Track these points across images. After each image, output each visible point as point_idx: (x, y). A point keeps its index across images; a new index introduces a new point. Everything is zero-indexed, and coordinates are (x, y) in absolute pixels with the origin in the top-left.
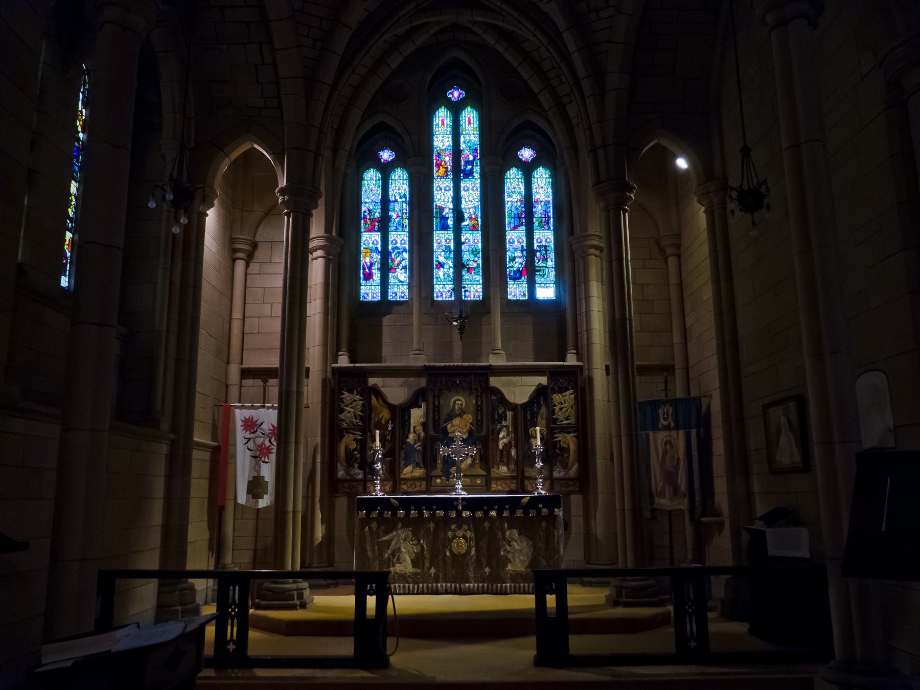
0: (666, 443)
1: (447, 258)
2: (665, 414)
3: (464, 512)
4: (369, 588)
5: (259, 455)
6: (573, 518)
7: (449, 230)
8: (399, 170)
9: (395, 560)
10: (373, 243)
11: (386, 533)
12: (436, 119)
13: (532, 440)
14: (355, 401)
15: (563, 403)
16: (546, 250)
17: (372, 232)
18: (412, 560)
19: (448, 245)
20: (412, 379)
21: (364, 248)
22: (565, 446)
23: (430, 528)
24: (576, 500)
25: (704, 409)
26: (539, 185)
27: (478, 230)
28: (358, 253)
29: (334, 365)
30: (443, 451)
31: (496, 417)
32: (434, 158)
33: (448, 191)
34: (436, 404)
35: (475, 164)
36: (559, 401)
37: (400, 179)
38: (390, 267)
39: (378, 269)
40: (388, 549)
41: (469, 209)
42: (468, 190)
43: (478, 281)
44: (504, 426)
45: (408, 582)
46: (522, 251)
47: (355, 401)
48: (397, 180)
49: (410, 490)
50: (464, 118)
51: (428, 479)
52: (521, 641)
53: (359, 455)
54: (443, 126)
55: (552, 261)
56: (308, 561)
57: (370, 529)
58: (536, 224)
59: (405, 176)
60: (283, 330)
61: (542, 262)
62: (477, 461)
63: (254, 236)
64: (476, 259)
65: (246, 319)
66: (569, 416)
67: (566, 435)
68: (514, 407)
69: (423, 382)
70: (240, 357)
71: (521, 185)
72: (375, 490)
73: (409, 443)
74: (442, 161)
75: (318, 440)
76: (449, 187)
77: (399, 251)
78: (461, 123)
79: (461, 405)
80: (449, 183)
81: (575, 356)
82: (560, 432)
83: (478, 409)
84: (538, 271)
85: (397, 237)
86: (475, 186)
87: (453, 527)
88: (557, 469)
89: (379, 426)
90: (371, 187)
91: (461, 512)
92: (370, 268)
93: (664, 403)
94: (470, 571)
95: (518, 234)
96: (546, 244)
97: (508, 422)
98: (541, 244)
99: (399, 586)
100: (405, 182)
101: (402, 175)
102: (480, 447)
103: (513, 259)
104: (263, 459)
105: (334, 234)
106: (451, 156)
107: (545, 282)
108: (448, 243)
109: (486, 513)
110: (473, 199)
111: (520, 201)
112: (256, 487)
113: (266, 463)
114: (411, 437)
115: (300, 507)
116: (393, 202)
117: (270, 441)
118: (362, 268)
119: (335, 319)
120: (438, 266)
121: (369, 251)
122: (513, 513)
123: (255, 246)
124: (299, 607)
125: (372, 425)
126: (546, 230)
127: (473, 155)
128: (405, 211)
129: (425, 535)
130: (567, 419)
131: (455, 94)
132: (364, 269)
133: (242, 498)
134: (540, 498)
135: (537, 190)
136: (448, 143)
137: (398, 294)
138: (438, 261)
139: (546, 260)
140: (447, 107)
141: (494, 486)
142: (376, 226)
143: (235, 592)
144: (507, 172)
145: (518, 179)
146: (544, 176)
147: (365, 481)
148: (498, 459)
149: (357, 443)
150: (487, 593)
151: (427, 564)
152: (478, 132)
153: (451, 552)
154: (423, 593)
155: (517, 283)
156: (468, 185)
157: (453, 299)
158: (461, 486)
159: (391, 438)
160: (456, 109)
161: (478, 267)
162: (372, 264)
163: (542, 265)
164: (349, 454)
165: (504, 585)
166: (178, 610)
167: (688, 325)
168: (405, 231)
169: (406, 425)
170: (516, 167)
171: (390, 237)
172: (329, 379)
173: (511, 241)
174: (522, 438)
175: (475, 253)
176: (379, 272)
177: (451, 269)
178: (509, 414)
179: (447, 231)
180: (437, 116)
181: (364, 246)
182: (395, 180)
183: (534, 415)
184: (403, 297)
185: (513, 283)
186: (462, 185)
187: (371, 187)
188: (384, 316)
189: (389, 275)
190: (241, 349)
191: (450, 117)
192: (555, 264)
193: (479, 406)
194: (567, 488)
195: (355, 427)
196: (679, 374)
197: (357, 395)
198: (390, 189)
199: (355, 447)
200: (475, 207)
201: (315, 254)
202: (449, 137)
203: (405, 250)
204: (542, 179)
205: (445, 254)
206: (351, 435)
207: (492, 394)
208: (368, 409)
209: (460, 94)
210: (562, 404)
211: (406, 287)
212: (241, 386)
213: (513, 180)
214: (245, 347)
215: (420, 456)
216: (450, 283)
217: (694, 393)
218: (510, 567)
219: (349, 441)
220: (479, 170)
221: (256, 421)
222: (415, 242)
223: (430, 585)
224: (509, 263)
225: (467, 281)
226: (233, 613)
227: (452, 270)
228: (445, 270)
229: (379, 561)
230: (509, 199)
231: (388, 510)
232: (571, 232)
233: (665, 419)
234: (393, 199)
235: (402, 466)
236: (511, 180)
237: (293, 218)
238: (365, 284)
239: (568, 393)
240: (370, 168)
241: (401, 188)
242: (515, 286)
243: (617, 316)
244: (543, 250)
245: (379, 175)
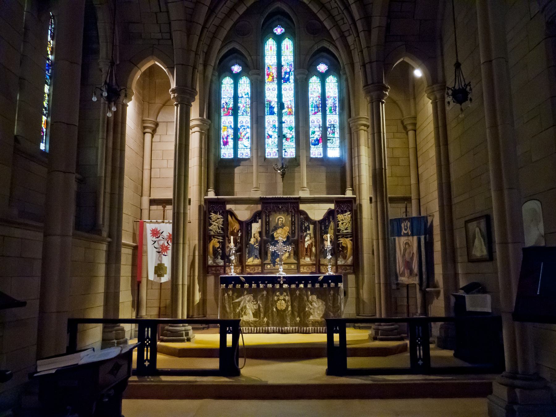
0: (406, 244)
2: (405, 226)
3: (284, 285)
4: (228, 329)
5: (161, 251)
6: (349, 289)
9: (243, 313)
10: (229, 123)
11: (238, 297)
13: (325, 242)
14: (218, 219)
15: (344, 220)
16: (334, 127)
18: (253, 314)
20: (253, 205)
22: (345, 245)
23: (264, 294)
24: (351, 278)
25: (429, 224)
27: (292, 115)
28: (219, 129)
29: (205, 197)
30: (272, 249)
31: (304, 228)
32: (266, 70)
34: (267, 221)
35: (291, 74)
36: (341, 219)
39: (232, 139)
40: (239, 306)
41: (287, 102)
42: (286, 90)
44: (308, 234)
45: (251, 326)
46: (319, 127)
47: (218, 219)
49: (252, 272)
50: (284, 45)
51: (263, 265)
52: (318, 360)
53: (221, 251)
56: (191, 314)
57: (228, 295)
59: (248, 82)
60: (175, 176)
62: (292, 255)
63: (156, 119)
64: (291, 132)
65: (152, 169)
66: (347, 228)
67: (345, 239)
68: (314, 223)
69: (259, 207)
70: (149, 192)
72: (231, 272)
73: (251, 244)
75: (197, 242)
76: (275, 88)
77: (244, 127)
78: (282, 48)
79: (283, 221)
80: (275, 86)
81: (351, 191)
82: (342, 237)
83: (293, 223)
84: (329, 140)
87: (278, 294)
88: (340, 260)
89: (233, 233)
90: (227, 88)
91: (282, 285)
92: (227, 138)
93: (405, 220)
94: (288, 320)
95: (317, 117)
97: (311, 231)
99: (246, 329)
100: (248, 85)
101: (246, 81)
102: (294, 246)
104: (163, 254)
105: (205, 117)
107: (333, 147)
108: (274, 123)
109: (297, 286)
111: (318, 97)
112: (159, 270)
113: (166, 255)
114: (252, 241)
115: (186, 283)
117: (168, 243)
119: (206, 169)
120: (269, 137)
121: (226, 128)
122: (313, 285)
123: (157, 125)
124: (186, 341)
125: (229, 233)
128: (248, 103)
129: (261, 298)
130: (346, 229)
131: (279, 31)
132: (223, 139)
133: (152, 276)
134: (330, 277)
135: (329, 90)
138: (268, 134)
139: (334, 133)
141: (302, 270)
142: (231, 113)
143: (148, 332)
145: (317, 83)
146: (333, 81)
147: (225, 267)
148: (305, 253)
149: (220, 244)
150: (298, 333)
151: (262, 315)
152: (293, 54)
153: (276, 308)
154: (260, 333)
156: (286, 87)
157: (277, 157)
158: (282, 270)
159: (241, 240)
160: (279, 40)
161: (292, 138)
162: (228, 136)
164: (215, 250)
165: (308, 328)
166: (115, 342)
167: (420, 173)
169: (249, 233)
170: (316, 76)
171: (239, 119)
172: (203, 206)
173: (313, 121)
174: (319, 241)
176: (232, 140)
178: (311, 227)
180: (267, 44)
183: (327, 227)
184: (247, 156)
188: (235, 168)
190: (149, 188)
192: (340, 136)
193: (293, 222)
194: (345, 270)
195: (219, 234)
196: (414, 202)
197: (219, 215)
198: (239, 90)
199: (218, 246)
201: (194, 130)
202: (274, 57)
203: (248, 127)
204: (332, 82)
206: (216, 239)
207: (301, 215)
208: (226, 223)
209: (282, 30)
210: (343, 220)
212: (150, 210)
213: (314, 83)
214: (151, 186)
215: (258, 252)
216: (275, 147)
217: (422, 215)
218: (311, 317)
219: (215, 243)
221: (159, 230)
222: (254, 123)
223: (264, 328)
224: (312, 135)
225: (286, 146)
226: (147, 344)
227: (276, 140)
229: (234, 313)
230: (312, 96)
231: (239, 284)
232: (350, 116)
233: (405, 230)
234: (241, 96)
235: (247, 258)
237: (180, 107)
239: (346, 214)
240: (227, 76)
242: (315, 149)
243: (377, 167)
245: (232, 81)
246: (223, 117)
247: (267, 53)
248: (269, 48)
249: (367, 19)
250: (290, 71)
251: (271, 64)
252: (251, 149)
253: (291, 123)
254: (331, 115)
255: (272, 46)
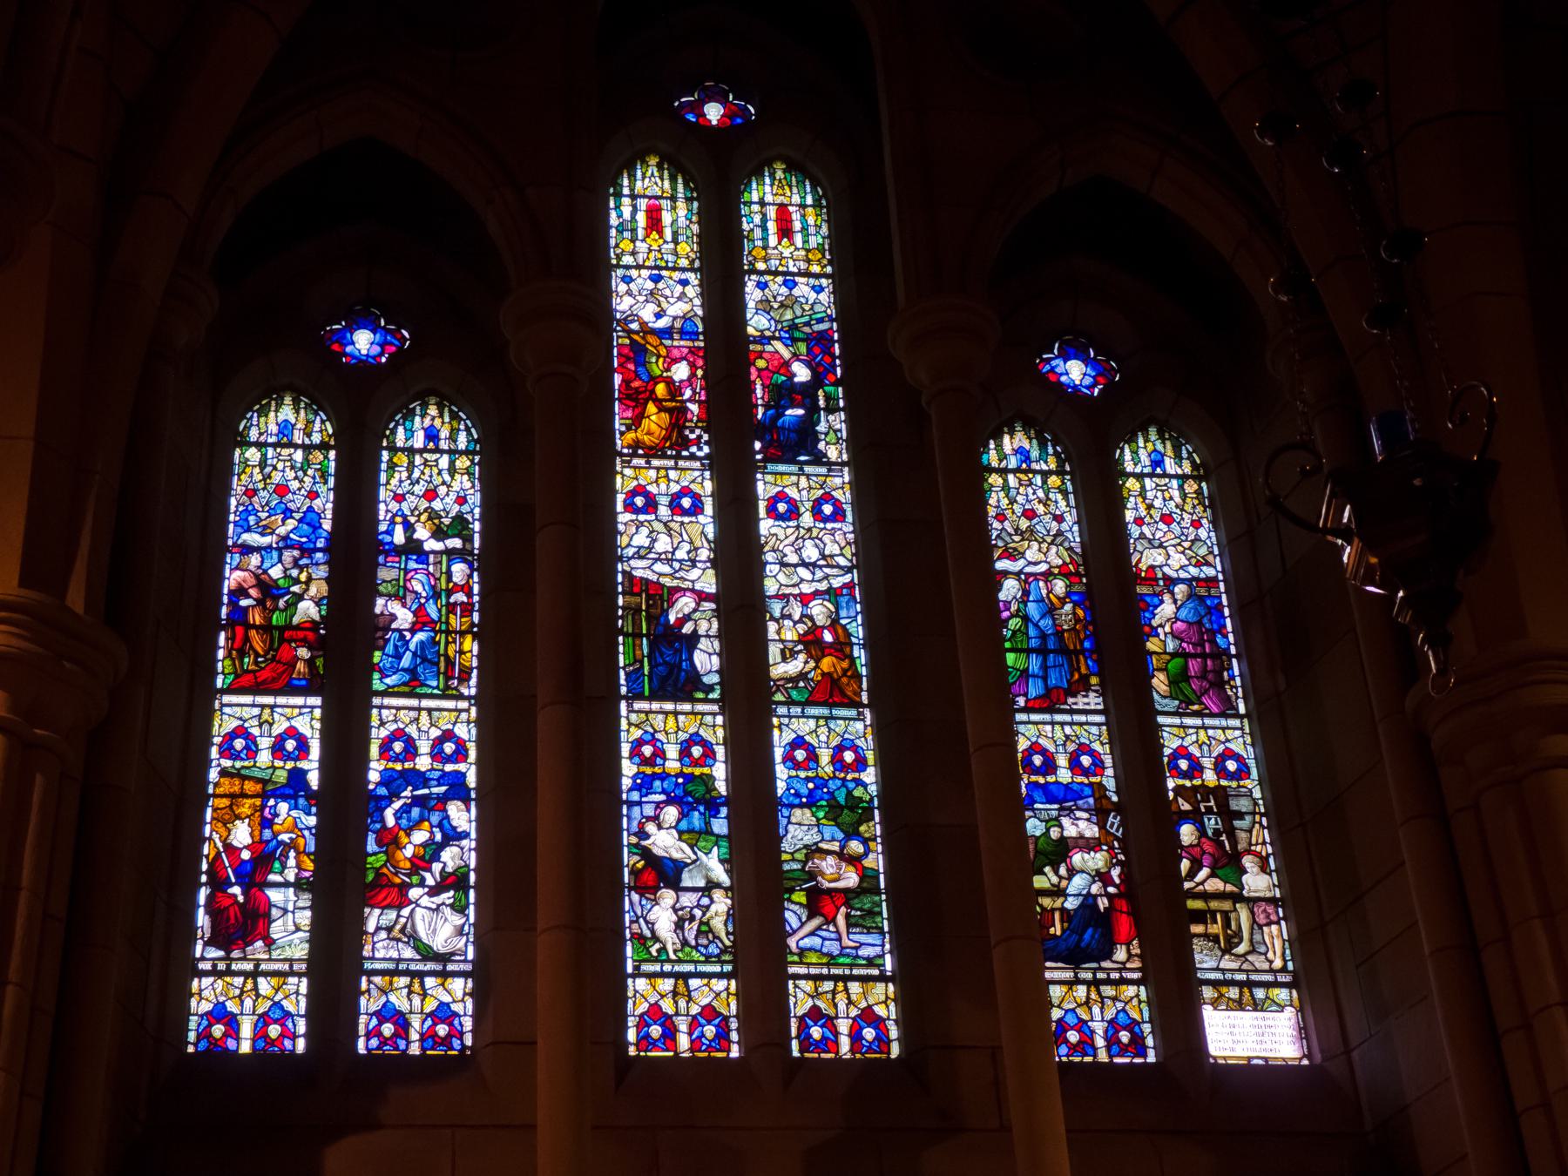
1: (692, 837)
7: (700, 695)
8: (433, 411)
10: (278, 749)
12: (617, 207)
16: (1229, 816)
17: (276, 693)
19: (697, 771)
21: (224, 773)
26: (1150, 507)
27: (857, 705)
33: (685, 512)
35: (822, 403)
37: (437, 450)
38: (371, 876)
39: (299, 885)
42: (793, 513)
43: (870, 962)
46: (1100, 814)
48: (421, 451)
50: (756, 208)
54: (655, 235)
55: (1264, 868)
58: (1160, 682)
61: (1213, 875)
64: (855, 847)
71: (1062, 504)
74: (655, 380)
76: (697, 499)
78: (745, 226)
84: (1200, 917)
85: (417, 719)
86: (827, 498)
92: (256, 870)
95: (1068, 730)
96: (1224, 783)
98: (1197, 782)
100: (463, 463)
101: (444, 433)
103: (1060, 851)
105: (76, 598)
106: (700, 363)
110: (824, 557)
116: (398, 551)
118: (204, 878)
120: (649, 878)
126: (1212, 715)
127: (808, 364)
128: (460, 597)
132: (218, 883)
135: (1145, 529)
136: (687, 307)
137: (416, 1022)
138: (646, 853)
139: (1229, 863)
140: (674, 165)
142: (300, 666)
144: (987, 445)
145: (1045, 475)
155: (1089, 976)
156: (792, 493)
162: (265, 856)
163: (1215, 885)
168: (461, 697)
171: (375, 721)
175: (847, 817)
176: (305, 900)
177: (718, 895)
179: (694, 701)
180: (626, 191)
181: (227, 763)
182: (411, 451)
185: (1068, 975)
186: (764, 488)
187: (277, 478)
189: (362, 921)
191: (689, 200)
200: (832, 594)
202: (684, 283)
203: (457, 788)
205: (683, 815)
211: (458, 985)
216: (717, 968)
220: (838, 421)
227: (721, 904)
228: (688, 900)
236: (1011, 477)
238: (221, 966)
241: (442, 490)
242: (1081, 991)
244: (1209, 811)
245: (322, 429)
246: (226, 699)
247: (626, 245)
248: (641, 218)
250: (817, 381)
251: (662, 323)
252: (483, 978)
253: (845, 767)
254: (1188, 721)
255: (665, 204)
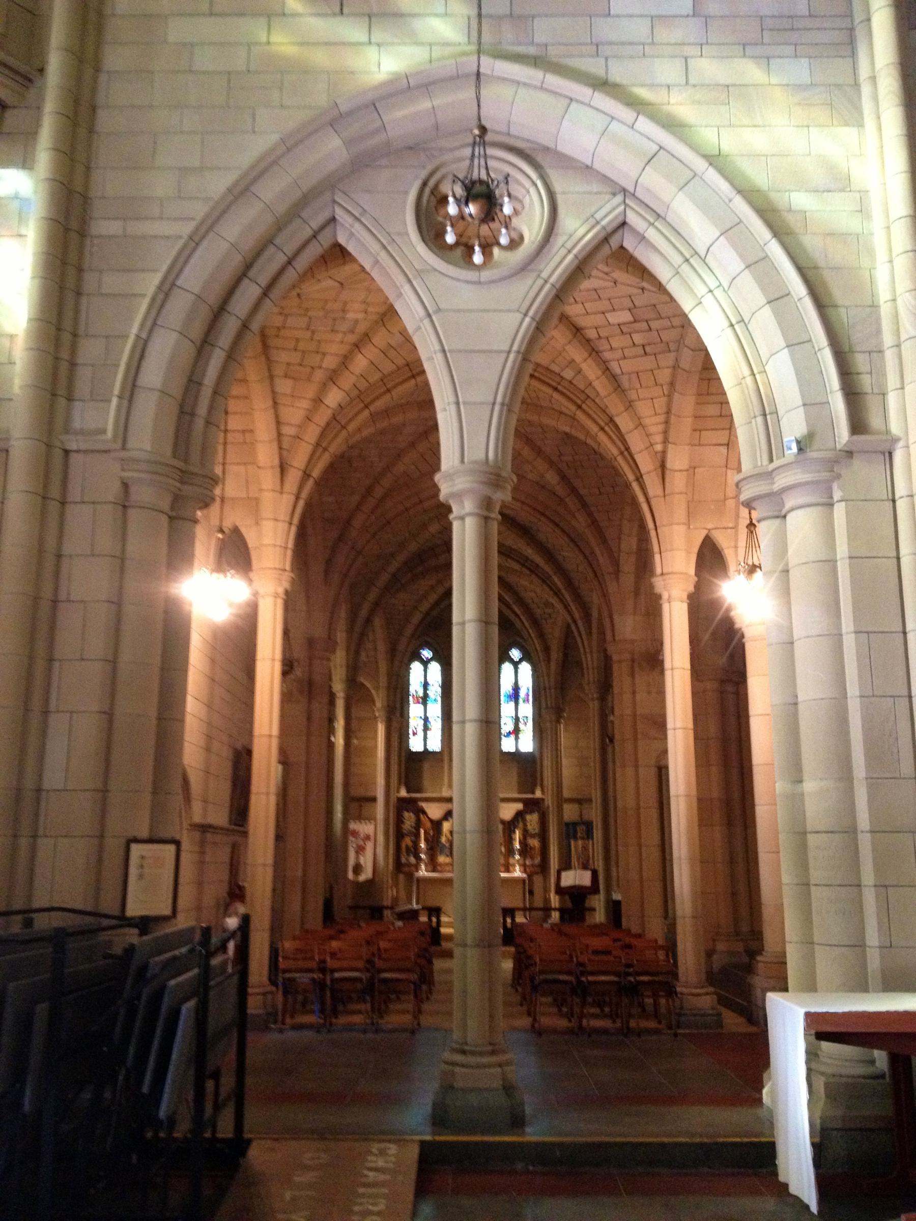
133: (351, 875)
204: (526, 669)
219: (408, 841)
249: (547, 649)
